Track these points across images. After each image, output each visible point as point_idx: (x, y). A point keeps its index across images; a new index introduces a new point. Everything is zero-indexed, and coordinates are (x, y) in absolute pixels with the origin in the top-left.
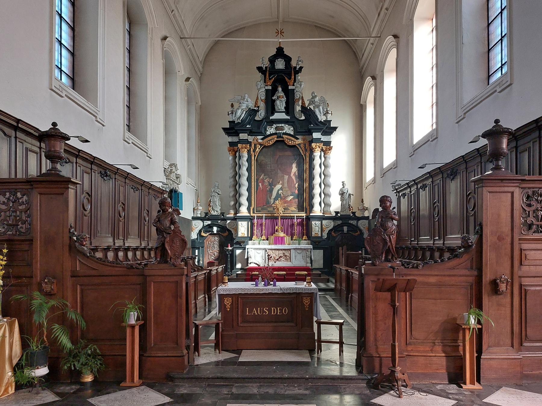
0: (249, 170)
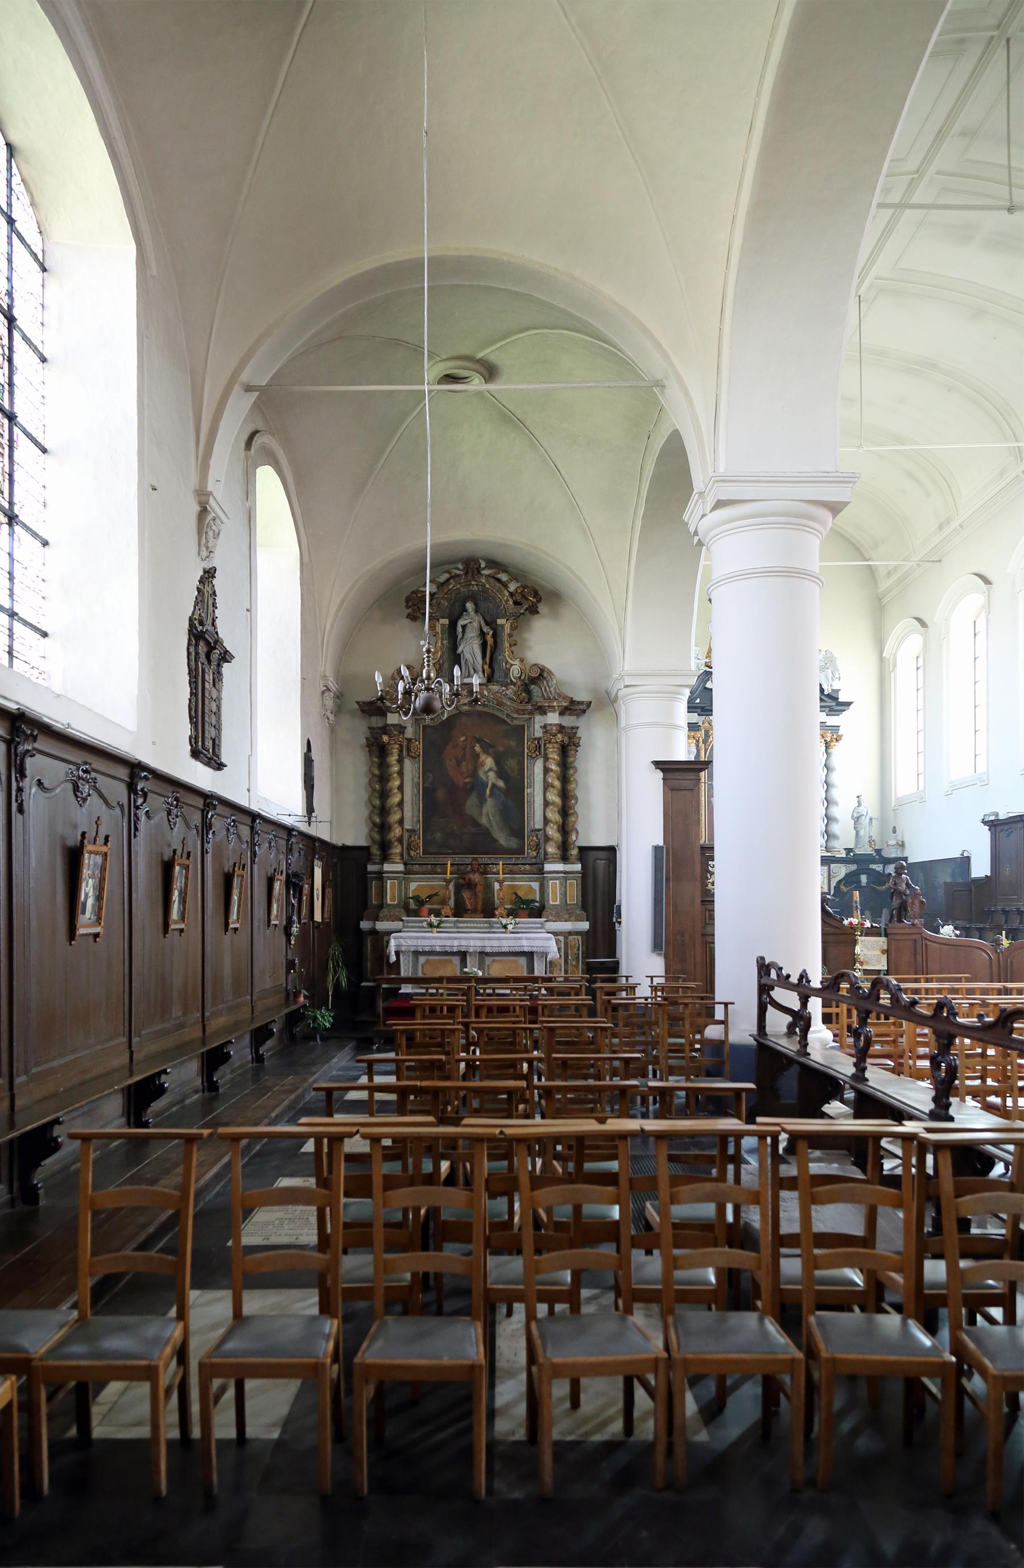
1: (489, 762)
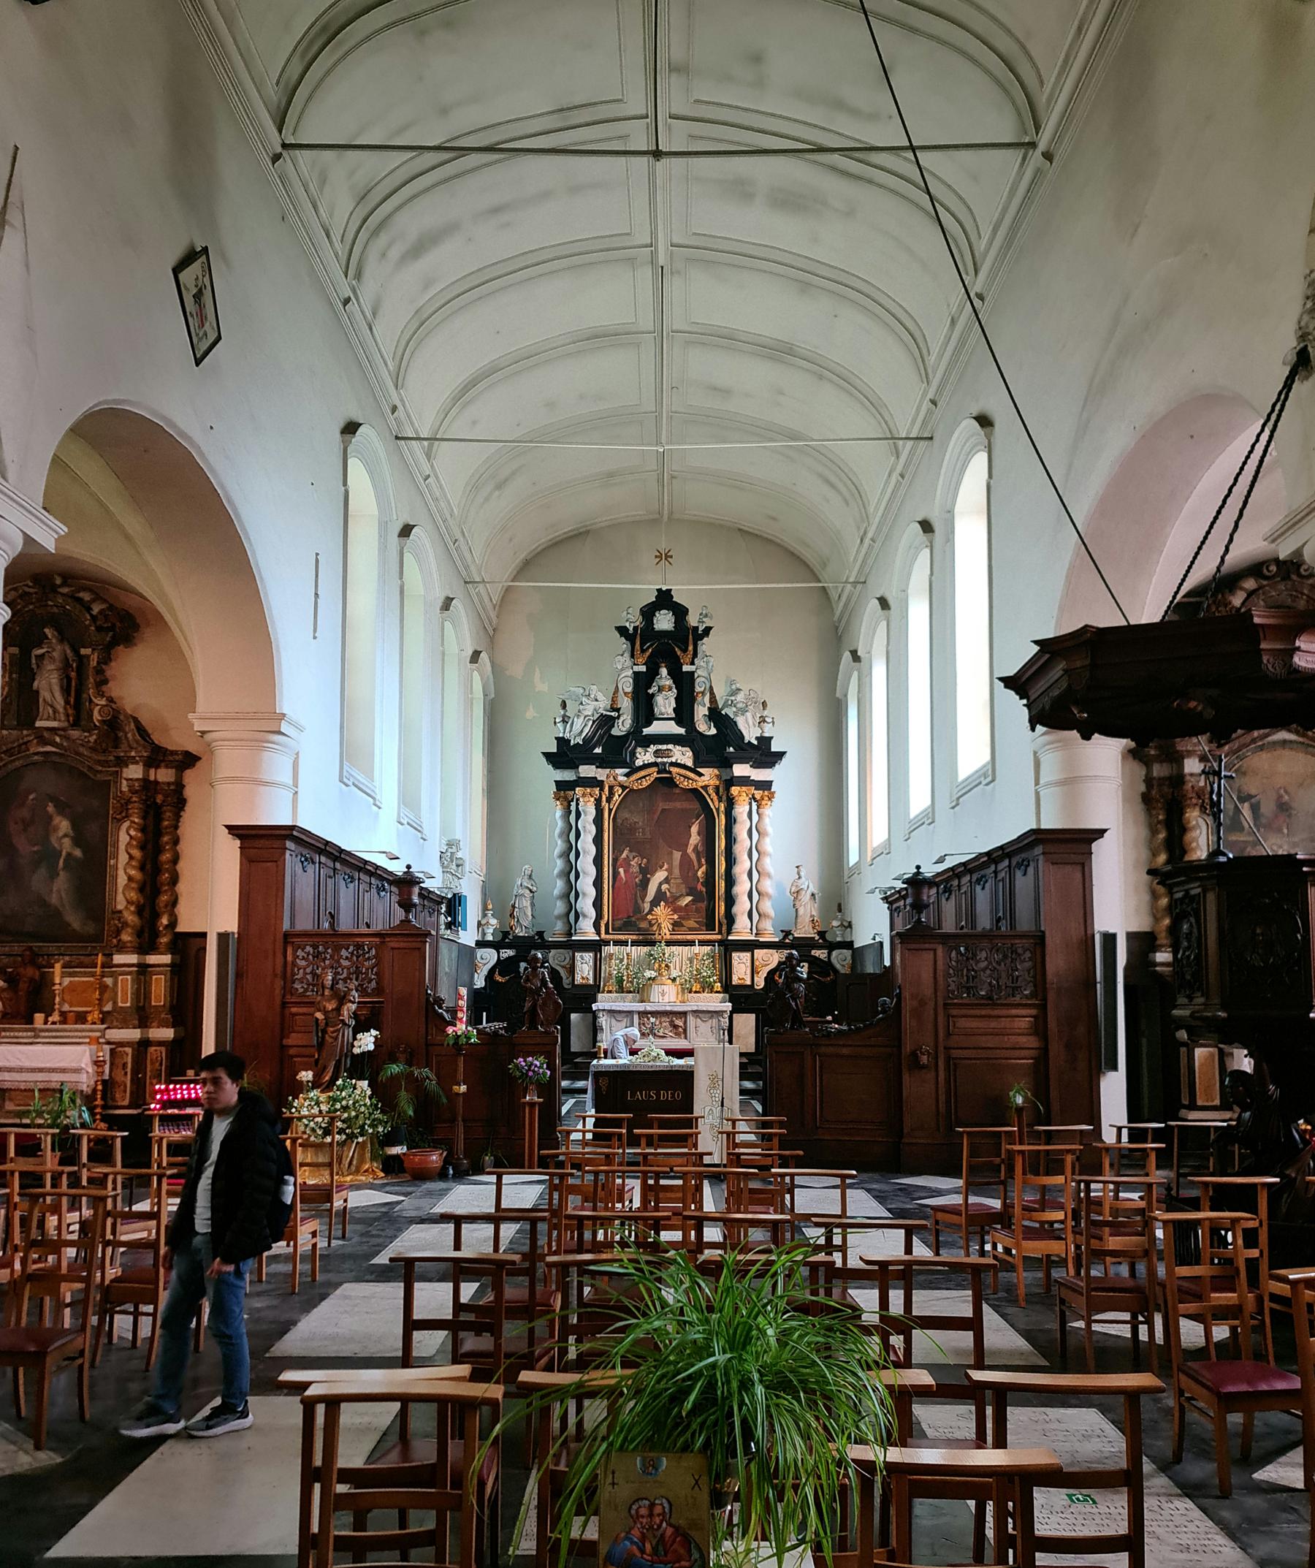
0: (598, 841)
1: (64, 825)
